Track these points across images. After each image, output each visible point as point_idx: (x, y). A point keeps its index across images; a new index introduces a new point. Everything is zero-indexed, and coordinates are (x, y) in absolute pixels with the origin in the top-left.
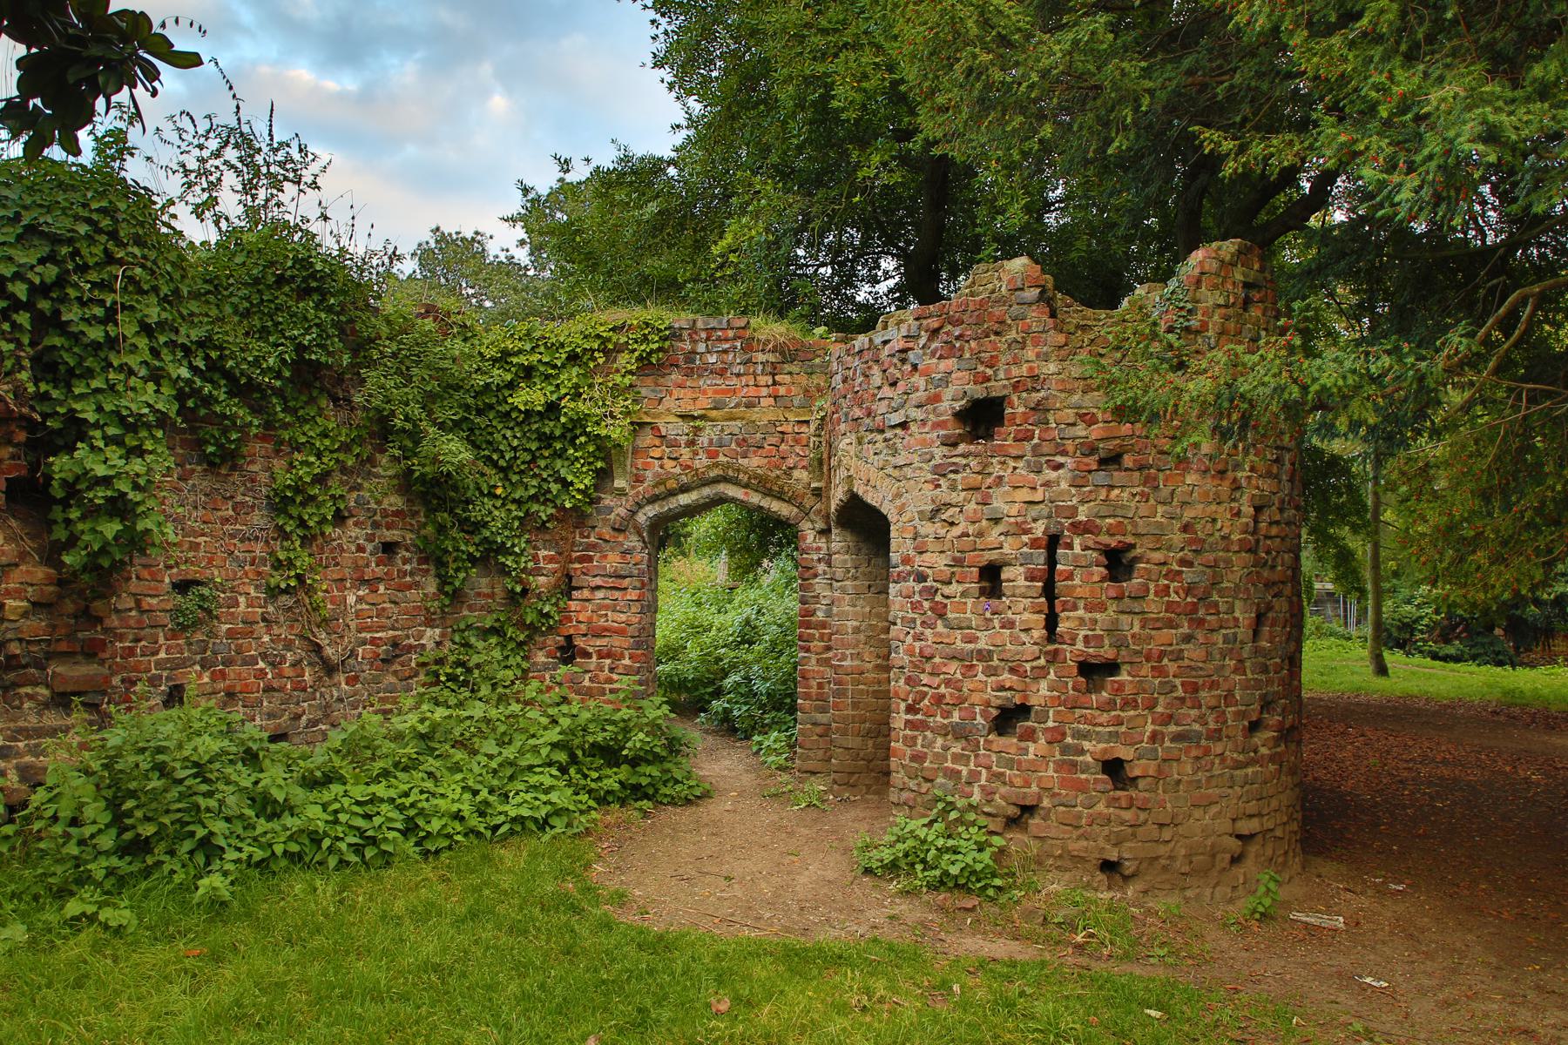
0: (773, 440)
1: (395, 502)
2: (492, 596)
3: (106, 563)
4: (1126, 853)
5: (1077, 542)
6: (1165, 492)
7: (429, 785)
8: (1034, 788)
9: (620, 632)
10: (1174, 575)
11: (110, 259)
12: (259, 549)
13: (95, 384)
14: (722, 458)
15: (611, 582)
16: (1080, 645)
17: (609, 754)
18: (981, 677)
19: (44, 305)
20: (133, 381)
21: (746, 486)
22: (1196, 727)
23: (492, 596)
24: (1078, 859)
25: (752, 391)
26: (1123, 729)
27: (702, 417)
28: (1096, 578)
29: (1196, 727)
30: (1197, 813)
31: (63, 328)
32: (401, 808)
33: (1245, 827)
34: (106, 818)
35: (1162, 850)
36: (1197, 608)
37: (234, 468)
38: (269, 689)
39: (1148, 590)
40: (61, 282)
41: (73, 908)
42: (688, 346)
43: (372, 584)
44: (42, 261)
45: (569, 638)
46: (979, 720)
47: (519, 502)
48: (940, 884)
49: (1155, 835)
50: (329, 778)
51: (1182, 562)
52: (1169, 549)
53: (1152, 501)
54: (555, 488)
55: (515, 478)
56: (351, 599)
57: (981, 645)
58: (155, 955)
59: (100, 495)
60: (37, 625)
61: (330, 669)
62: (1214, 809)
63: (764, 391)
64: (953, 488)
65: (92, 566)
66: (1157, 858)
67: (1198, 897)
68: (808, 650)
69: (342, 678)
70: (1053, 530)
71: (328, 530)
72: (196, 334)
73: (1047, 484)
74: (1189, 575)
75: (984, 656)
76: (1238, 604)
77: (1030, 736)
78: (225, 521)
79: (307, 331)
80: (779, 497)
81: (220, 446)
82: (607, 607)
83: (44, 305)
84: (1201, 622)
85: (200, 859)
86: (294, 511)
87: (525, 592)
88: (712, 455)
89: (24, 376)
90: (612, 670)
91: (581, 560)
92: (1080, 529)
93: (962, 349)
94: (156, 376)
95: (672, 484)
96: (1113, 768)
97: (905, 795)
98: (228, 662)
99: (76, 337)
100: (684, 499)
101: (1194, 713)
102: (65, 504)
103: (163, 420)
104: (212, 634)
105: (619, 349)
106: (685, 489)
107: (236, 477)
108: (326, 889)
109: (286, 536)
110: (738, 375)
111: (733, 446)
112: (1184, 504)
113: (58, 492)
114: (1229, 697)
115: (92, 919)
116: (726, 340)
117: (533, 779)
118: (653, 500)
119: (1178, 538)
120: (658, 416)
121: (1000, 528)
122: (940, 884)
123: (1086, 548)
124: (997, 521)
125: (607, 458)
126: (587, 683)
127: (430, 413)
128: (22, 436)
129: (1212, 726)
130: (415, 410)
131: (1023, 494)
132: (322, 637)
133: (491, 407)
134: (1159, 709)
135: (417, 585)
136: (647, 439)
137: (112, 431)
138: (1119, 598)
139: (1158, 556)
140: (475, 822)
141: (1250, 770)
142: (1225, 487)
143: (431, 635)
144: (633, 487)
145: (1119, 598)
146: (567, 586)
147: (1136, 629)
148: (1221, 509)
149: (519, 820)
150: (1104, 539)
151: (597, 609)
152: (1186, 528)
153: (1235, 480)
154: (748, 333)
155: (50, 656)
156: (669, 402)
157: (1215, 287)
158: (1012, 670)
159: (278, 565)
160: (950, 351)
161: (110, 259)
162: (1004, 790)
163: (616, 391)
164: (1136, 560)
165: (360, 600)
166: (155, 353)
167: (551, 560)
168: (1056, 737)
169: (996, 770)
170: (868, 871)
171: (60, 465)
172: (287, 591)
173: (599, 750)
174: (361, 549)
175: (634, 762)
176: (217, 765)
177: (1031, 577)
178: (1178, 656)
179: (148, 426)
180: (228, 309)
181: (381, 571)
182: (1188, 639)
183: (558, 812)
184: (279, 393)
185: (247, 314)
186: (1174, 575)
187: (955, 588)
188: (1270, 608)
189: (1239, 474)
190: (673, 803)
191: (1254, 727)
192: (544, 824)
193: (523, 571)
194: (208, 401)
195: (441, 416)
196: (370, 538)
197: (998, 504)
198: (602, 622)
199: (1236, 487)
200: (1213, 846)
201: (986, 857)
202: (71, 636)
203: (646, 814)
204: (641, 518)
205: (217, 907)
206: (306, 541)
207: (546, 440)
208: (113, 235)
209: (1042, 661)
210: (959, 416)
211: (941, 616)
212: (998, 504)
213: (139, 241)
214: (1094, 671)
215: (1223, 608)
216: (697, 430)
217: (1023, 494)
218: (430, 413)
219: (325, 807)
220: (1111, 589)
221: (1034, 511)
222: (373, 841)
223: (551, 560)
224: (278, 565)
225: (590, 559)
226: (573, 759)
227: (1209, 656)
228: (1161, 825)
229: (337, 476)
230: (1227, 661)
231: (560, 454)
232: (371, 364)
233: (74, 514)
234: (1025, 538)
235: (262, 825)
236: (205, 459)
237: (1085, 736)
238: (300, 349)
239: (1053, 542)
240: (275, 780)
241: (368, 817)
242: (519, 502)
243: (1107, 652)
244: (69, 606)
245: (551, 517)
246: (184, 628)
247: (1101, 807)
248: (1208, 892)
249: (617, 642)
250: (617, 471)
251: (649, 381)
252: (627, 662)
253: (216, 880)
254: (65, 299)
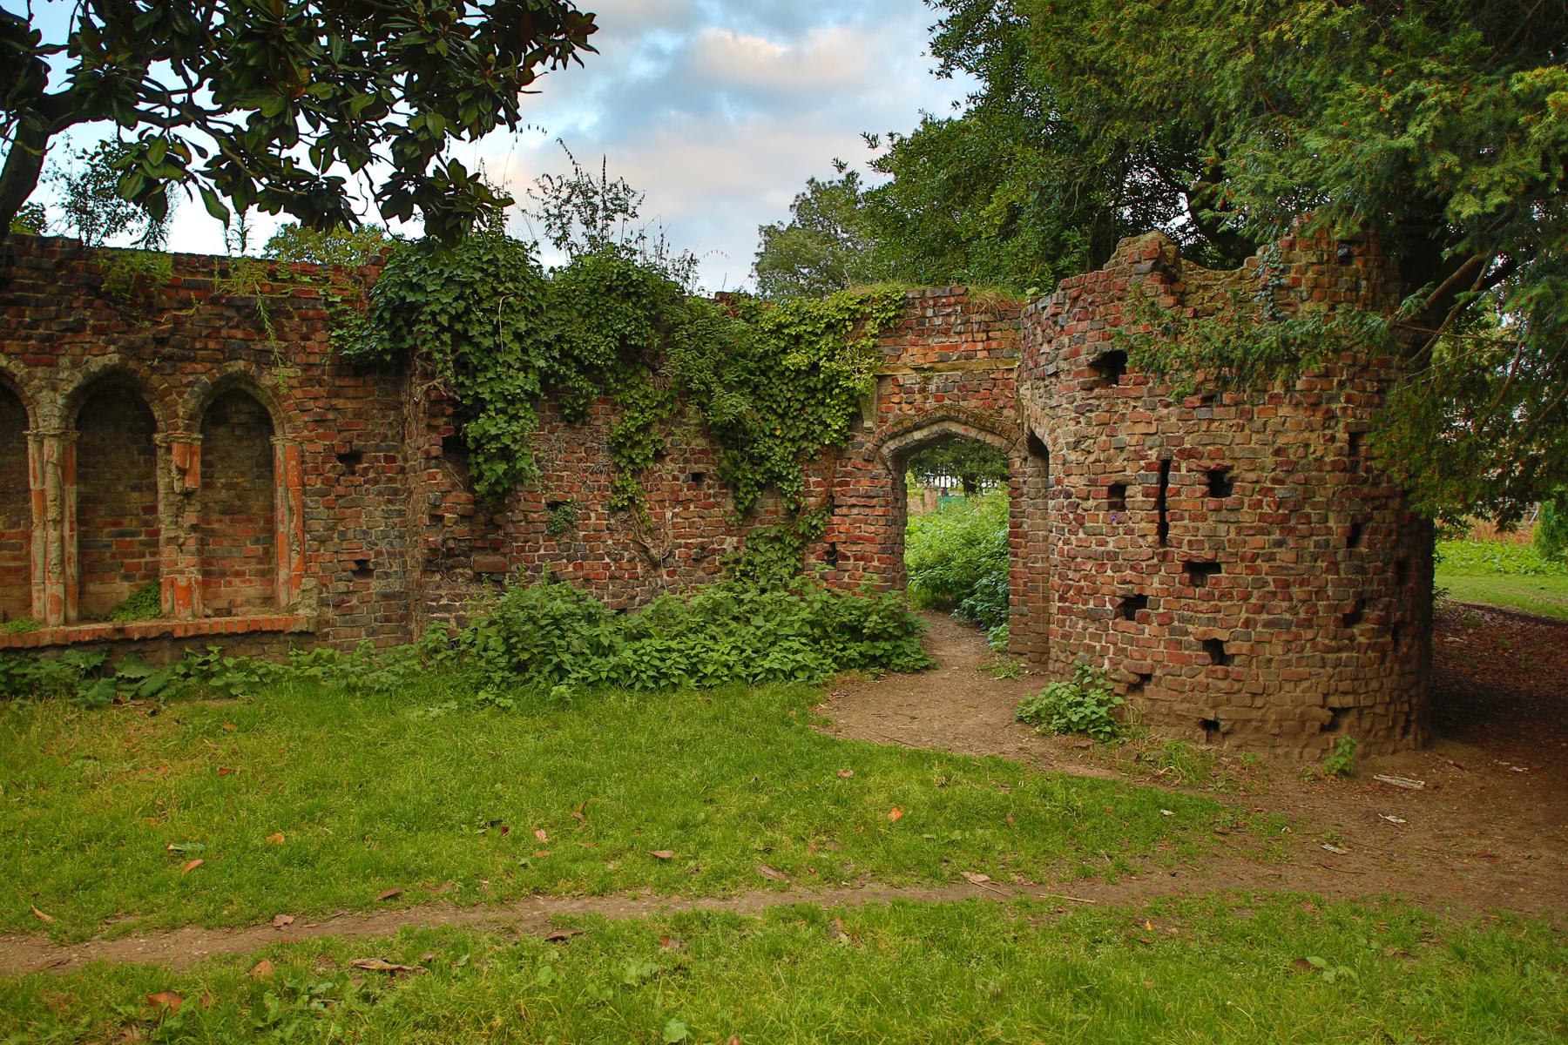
0: (987, 385)
1: (700, 443)
2: (776, 512)
3: (499, 489)
4: (1223, 715)
5: (1184, 465)
6: (1258, 423)
7: (710, 643)
8: (1149, 661)
9: (872, 541)
10: (1266, 492)
11: (496, 293)
12: (603, 480)
13: (490, 375)
14: (947, 402)
16: (1185, 548)
17: (854, 631)
18: (1109, 572)
19: (458, 327)
20: (512, 372)
21: (965, 423)
22: (1287, 616)
23: (776, 512)
24: (1181, 718)
26: (1221, 616)
27: (930, 369)
28: (1198, 494)
29: (1287, 616)
30: (1288, 687)
31: (469, 340)
32: (688, 657)
33: (1335, 701)
34: (502, 648)
35: (1256, 714)
36: (1290, 517)
37: (584, 423)
38: (612, 577)
39: (1242, 504)
40: (468, 311)
41: (482, 695)
42: (919, 312)
43: (685, 504)
44: (456, 299)
45: (833, 544)
46: (1109, 606)
47: (793, 440)
48: (1068, 728)
49: (1248, 702)
50: (642, 634)
51: (1275, 481)
52: (1263, 469)
53: (1247, 431)
54: (818, 429)
55: (789, 422)
56: (669, 515)
57: (1111, 547)
58: (520, 722)
59: (493, 447)
60: (463, 529)
61: (655, 565)
62: (1305, 684)
63: (980, 346)
64: (1089, 424)
65: (491, 492)
66: (1250, 721)
67: (1287, 755)
68: (1016, 555)
69: (664, 571)
70: (1164, 456)
71: (650, 465)
72: (552, 334)
73: (1159, 419)
74: (1280, 491)
75: (1112, 556)
76: (1331, 516)
77: (1145, 619)
78: (580, 460)
79: (628, 324)
80: (992, 431)
81: (573, 409)
82: (860, 521)
83: (458, 327)
84: (1292, 530)
85: (556, 677)
86: (625, 452)
87: (798, 509)
88: (939, 399)
89: (448, 373)
90: (864, 570)
91: (840, 484)
92: (1189, 454)
93: (1093, 313)
94: (526, 367)
95: (907, 424)
96: (1215, 649)
97: (1058, 665)
98: (585, 558)
99: (478, 345)
100: (918, 435)
101: (1285, 604)
102: (475, 452)
103: (532, 397)
104: (574, 539)
105: (866, 317)
106: (918, 427)
107: (586, 430)
108: (630, 700)
109: (622, 470)
110: (959, 333)
112: (1275, 433)
113: (472, 445)
114: (1320, 592)
115: (492, 702)
116: (950, 305)
117: (787, 644)
118: (894, 436)
119: (1269, 461)
120: (897, 369)
121: (1124, 456)
122: (1068, 728)
123: (1189, 470)
124: (1122, 449)
125: (857, 405)
126: (846, 580)
127: (720, 377)
128: (450, 411)
129: (1302, 615)
130: (708, 375)
131: (1141, 428)
132: (648, 542)
133: (771, 368)
134: (1253, 601)
135: (718, 505)
136: (888, 388)
137: (499, 405)
138: (1218, 510)
139: (1252, 476)
140: (739, 669)
141: (1344, 655)
142: (1318, 418)
143: (730, 542)
145: (1218, 510)
146: (830, 504)
147: (1232, 535)
148: (1314, 436)
149: (770, 670)
150: (1206, 463)
151: (856, 523)
152: (1277, 452)
153: (1328, 411)
154: (966, 299)
155: (472, 549)
156: (905, 358)
157: (1309, 248)
158: (1132, 568)
159: (616, 491)
160: (1087, 315)
161: (496, 293)
162: (1126, 661)
163: (865, 352)
164: (1233, 479)
165: (675, 515)
166: (525, 351)
167: (818, 484)
168: (1166, 621)
169: (1115, 648)
170: (1021, 720)
171: (472, 429)
172: (622, 509)
173: (843, 628)
174: (675, 478)
175: (874, 637)
176: (568, 621)
177: (1146, 495)
178: (1271, 558)
179: (521, 400)
180: (575, 314)
181: (690, 494)
182: (1279, 544)
183: (803, 668)
184: (612, 369)
185: (588, 315)
186: (1266, 492)
187: (1091, 503)
188: (1369, 518)
189: (1334, 406)
190: (902, 670)
191: (1350, 620)
192: (791, 675)
193: (797, 492)
194: (564, 378)
195: (728, 377)
196: (682, 470)
197: (1123, 436)
198: (857, 532)
199: (1330, 416)
200: (1302, 714)
201: (1103, 711)
202: (483, 537)
203: (877, 677)
204: (885, 451)
205: (561, 702)
206: (635, 473)
207: (811, 391)
208: (496, 276)
209: (1155, 561)
210: (1093, 366)
211: (1082, 525)
212: (1123, 436)
213: (513, 279)
214: (1199, 570)
215: (1314, 518)
216: (927, 380)
217: (1141, 428)
218: (720, 377)
219: (635, 652)
220: (1212, 502)
221: (1149, 441)
222: (665, 676)
223: (818, 484)
224: (616, 491)
225: (848, 484)
226: (826, 635)
227: (1299, 558)
228: (1254, 695)
229: (657, 426)
230: (1319, 563)
231: (822, 403)
232: (676, 345)
233: (481, 459)
234: (1142, 463)
235: (595, 660)
236: (565, 418)
237: (1190, 620)
238: (624, 337)
239: (1165, 466)
240: (604, 632)
241: (663, 660)
242: (793, 440)
243: (1207, 554)
244: (481, 518)
245: (817, 452)
246: (555, 534)
247: (1201, 677)
248: (1297, 751)
249: (868, 547)
250: (865, 414)
251: (890, 341)
252: (876, 563)
253: (563, 688)
254: (470, 322)
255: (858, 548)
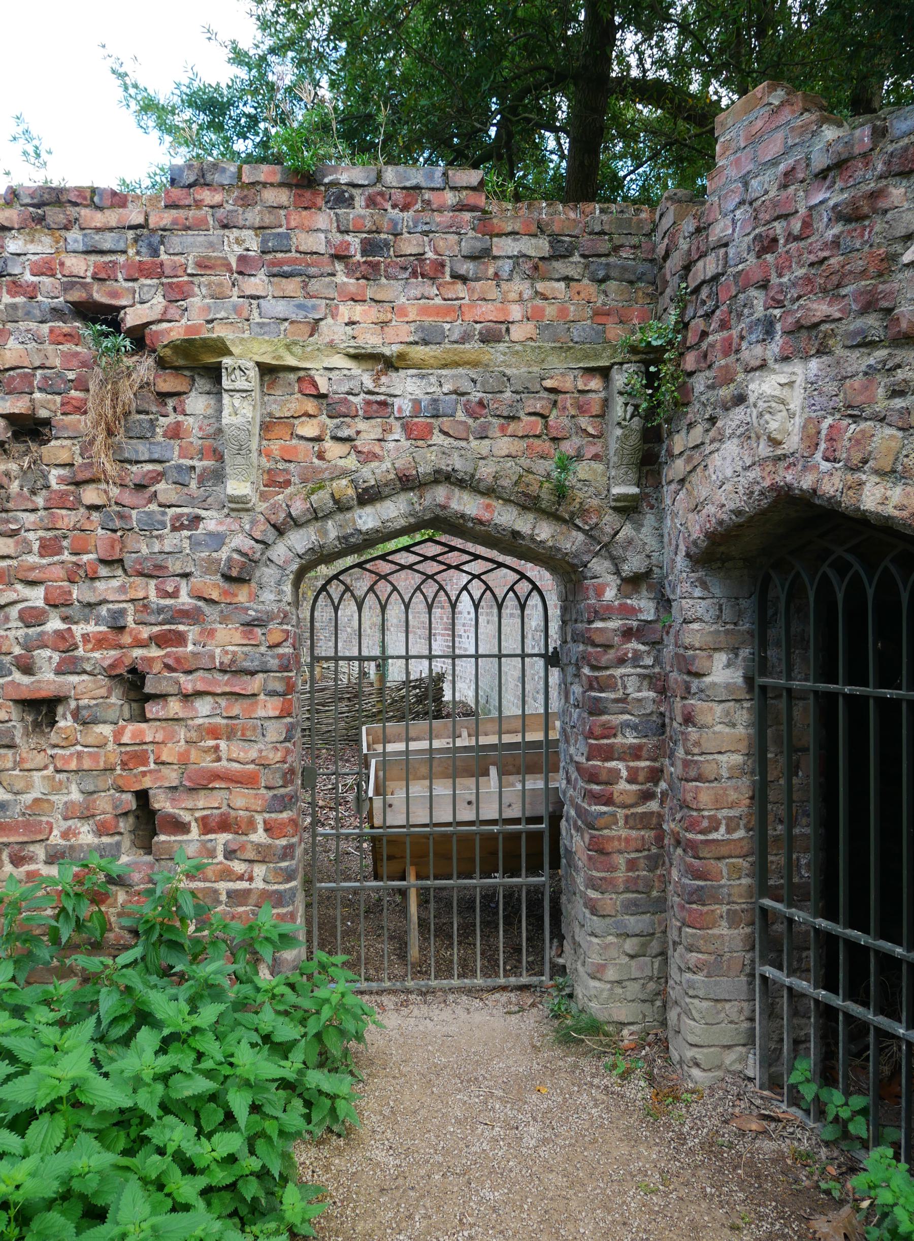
9: (247, 781)
15: (222, 683)
25: (488, 312)
82: (214, 732)
90: (230, 854)
111: (461, 416)
144: (263, 497)
198: (207, 763)
249: (241, 800)
252: (259, 836)
255: (202, 801)
